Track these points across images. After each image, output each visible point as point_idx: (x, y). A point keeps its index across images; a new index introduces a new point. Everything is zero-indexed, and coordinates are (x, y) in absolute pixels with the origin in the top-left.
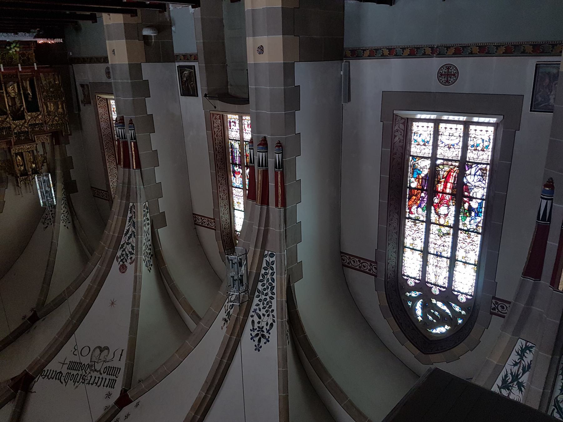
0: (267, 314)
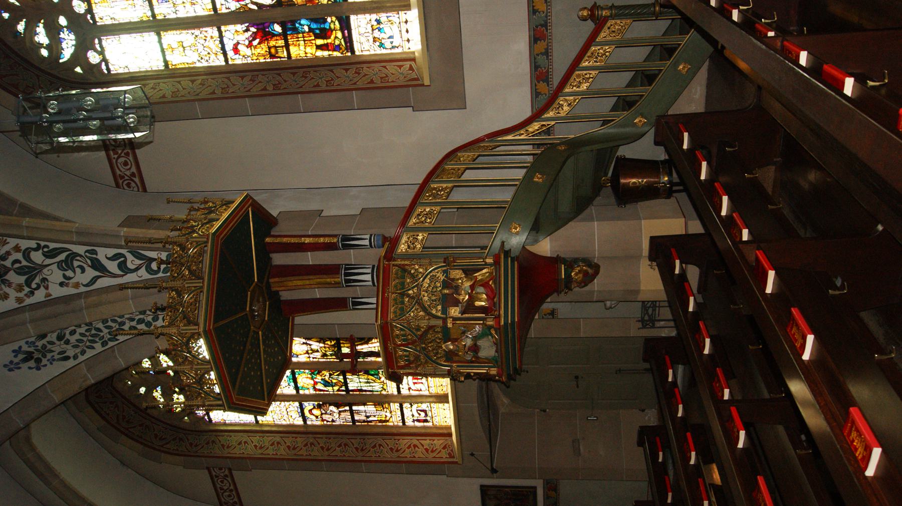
0: (77, 344)
